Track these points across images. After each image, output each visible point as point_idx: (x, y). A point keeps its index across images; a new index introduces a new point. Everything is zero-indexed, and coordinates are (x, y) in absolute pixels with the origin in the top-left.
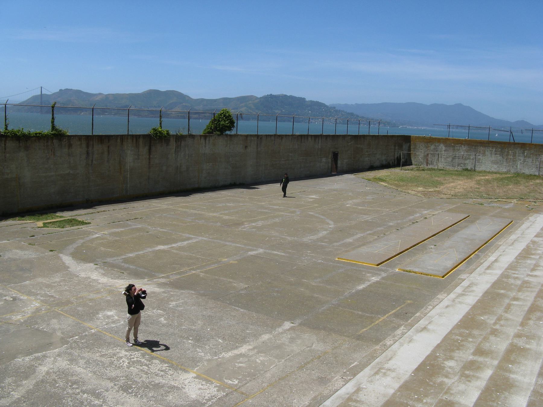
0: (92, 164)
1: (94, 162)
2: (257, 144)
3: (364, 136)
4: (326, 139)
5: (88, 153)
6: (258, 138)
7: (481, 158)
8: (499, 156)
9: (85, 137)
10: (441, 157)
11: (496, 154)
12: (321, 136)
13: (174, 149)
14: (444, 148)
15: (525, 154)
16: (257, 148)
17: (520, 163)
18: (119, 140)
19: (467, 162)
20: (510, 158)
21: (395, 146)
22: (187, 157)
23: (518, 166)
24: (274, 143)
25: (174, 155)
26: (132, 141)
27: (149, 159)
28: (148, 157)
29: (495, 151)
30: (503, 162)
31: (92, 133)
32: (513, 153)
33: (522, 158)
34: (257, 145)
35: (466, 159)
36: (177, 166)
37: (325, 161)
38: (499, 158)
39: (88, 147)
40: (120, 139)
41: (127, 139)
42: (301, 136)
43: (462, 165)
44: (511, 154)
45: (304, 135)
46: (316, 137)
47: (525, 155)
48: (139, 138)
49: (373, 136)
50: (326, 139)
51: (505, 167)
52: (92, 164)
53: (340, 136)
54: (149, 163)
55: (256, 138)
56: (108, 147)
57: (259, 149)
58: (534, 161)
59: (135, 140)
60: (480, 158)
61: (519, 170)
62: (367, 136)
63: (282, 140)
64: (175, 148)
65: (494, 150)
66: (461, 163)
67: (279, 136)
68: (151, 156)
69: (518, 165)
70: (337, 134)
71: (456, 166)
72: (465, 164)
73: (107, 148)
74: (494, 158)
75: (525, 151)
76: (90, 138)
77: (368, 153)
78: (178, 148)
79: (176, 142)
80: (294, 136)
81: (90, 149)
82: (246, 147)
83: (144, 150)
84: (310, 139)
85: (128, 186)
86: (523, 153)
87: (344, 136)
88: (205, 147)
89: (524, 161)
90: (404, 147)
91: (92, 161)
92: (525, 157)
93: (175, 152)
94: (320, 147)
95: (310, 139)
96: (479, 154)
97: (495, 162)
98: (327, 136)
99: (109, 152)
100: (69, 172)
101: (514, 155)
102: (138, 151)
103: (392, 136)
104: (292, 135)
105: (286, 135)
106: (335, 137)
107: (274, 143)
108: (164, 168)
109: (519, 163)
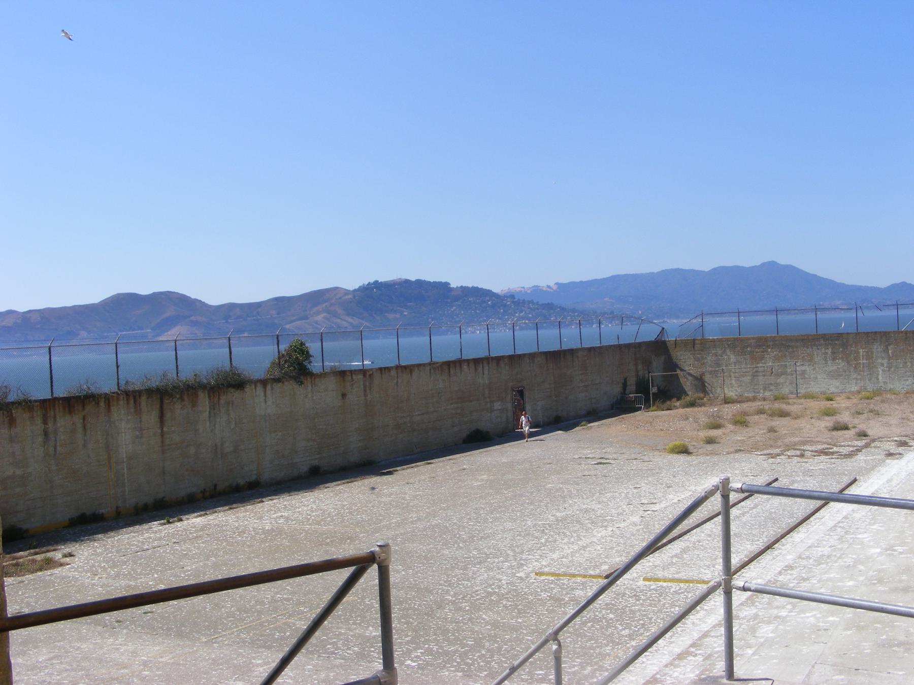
0: (55, 455)
1: (58, 448)
2: (365, 387)
3: (572, 352)
4: (498, 364)
5: (46, 433)
6: (364, 375)
7: (808, 369)
8: (840, 361)
9: (38, 403)
10: (730, 376)
11: (834, 359)
12: (488, 360)
13: (208, 413)
14: (733, 358)
15: (890, 352)
16: (365, 395)
17: (883, 371)
18: (102, 404)
19: (781, 380)
20: (863, 364)
21: (636, 365)
22: (233, 426)
23: (880, 378)
24: (397, 382)
25: (208, 423)
26: (128, 403)
27: (162, 434)
28: (160, 431)
29: (833, 353)
30: (850, 372)
31: (52, 395)
32: (867, 352)
33: (885, 362)
34: (365, 391)
35: (779, 375)
36: (216, 445)
37: (500, 408)
38: (842, 364)
39: (45, 422)
40: (105, 402)
41: (118, 399)
42: (448, 364)
43: (772, 387)
44: (863, 356)
45: (454, 362)
46: (477, 362)
47: (889, 355)
48: (140, 396)
49: (590, 350)
50: (498, 364)
51: (855, 381)
52: (55, 455)
53: (524, 355)
54: (163, 442)
55: (361, 376)
56: (84, 419)
57: (369, 397)
58: (909, 364)
59: (132, 402)
60: (804, 370)
61: (882, 385)
62: (577, 350)
63: (411, 374)
64: (208, 410)
65: (829, 351)
66: (771, 384)
67: (405, 368)
68: (165, 429)
69: (878, 375)
70: (518, 352)
71: (762, 391)
72: (777, 384)
73: (82, 421)
74: (832, 367)
75: (889, 348)
76: (48, 404)
77: (583, 384)
78: (214, 409)
79: (209, 397)
80: (435, 366)
81: (50, 425)
82: (344, 395)
83: (150, 418)
84: (465, 367)
85: (127, 489)
86: (886, 350)
87: (532, 356)
88: (266, 402)
89: (889, 367)
90: (654, 364)
91: (55, 448)
92: (889, 358)
93: (210, 417)
94: (487, 382)
95: (465, 367)
96: (802, 363)
97: (835, 375)
98: (498, 359)
99: (84, 427)
100: (14, 473)
101: (869, 356)
102: (141, 422)
103: (628, 346)
104: (431, 364)
105: (419, 366)
106: (514, 359)
107: (397, 382)
108: (192, 450)
109: (881, 372)
